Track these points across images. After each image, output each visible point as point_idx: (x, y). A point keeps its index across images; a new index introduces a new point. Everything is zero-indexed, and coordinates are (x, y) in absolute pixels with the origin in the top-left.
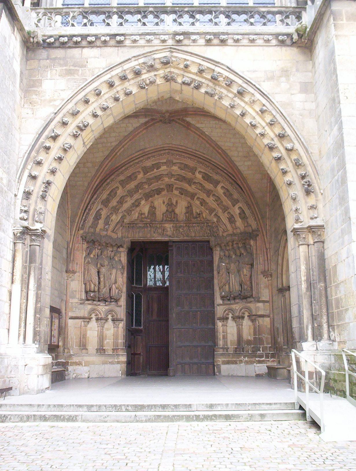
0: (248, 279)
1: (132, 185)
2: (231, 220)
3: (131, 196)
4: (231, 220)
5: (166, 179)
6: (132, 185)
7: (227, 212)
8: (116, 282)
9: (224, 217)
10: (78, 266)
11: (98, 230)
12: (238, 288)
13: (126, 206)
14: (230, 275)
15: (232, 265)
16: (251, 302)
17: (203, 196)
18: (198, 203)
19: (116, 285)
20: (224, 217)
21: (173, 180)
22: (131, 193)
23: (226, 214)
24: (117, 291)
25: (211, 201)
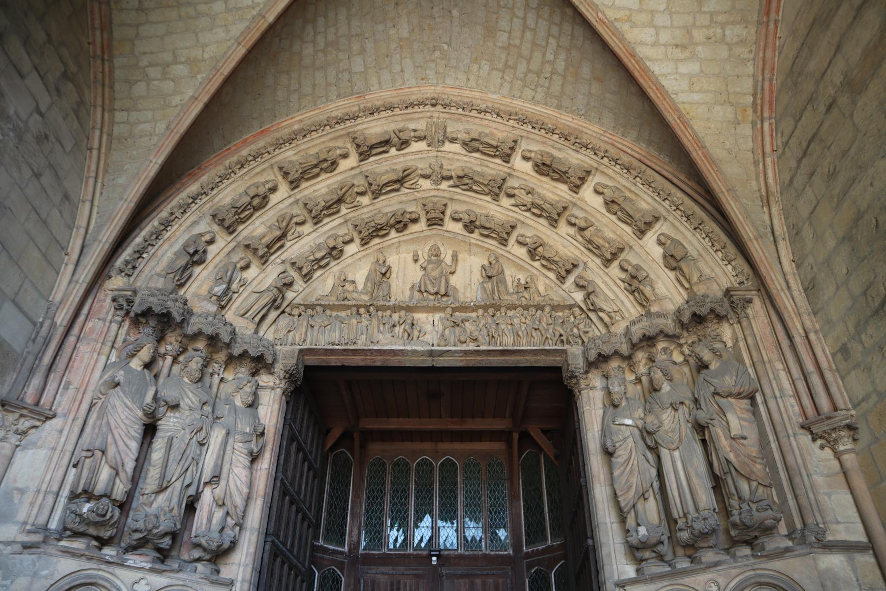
0: (754, 451)
1: (320, 188)
2: (635, 282)
3: (317, 220)
4: (635, 282)
5: (425, 184)
6: (320, 188)
7: (616, 263)
8: (215, 479)
9: (608, 283)
10: (71, 392)
11: (190, 291)
12: (706, 498)
13: (298, 248)
14: (665, 453)
15: (667, 417)
16: (781, 553)
17: (535, 228)
18: (522, 252)
19: (219, 491)
20: (608, 283)
21: (445, 185)
22: (318, 214)
23: (614, 269)
24: (219, 514)
25: (562, 241)
